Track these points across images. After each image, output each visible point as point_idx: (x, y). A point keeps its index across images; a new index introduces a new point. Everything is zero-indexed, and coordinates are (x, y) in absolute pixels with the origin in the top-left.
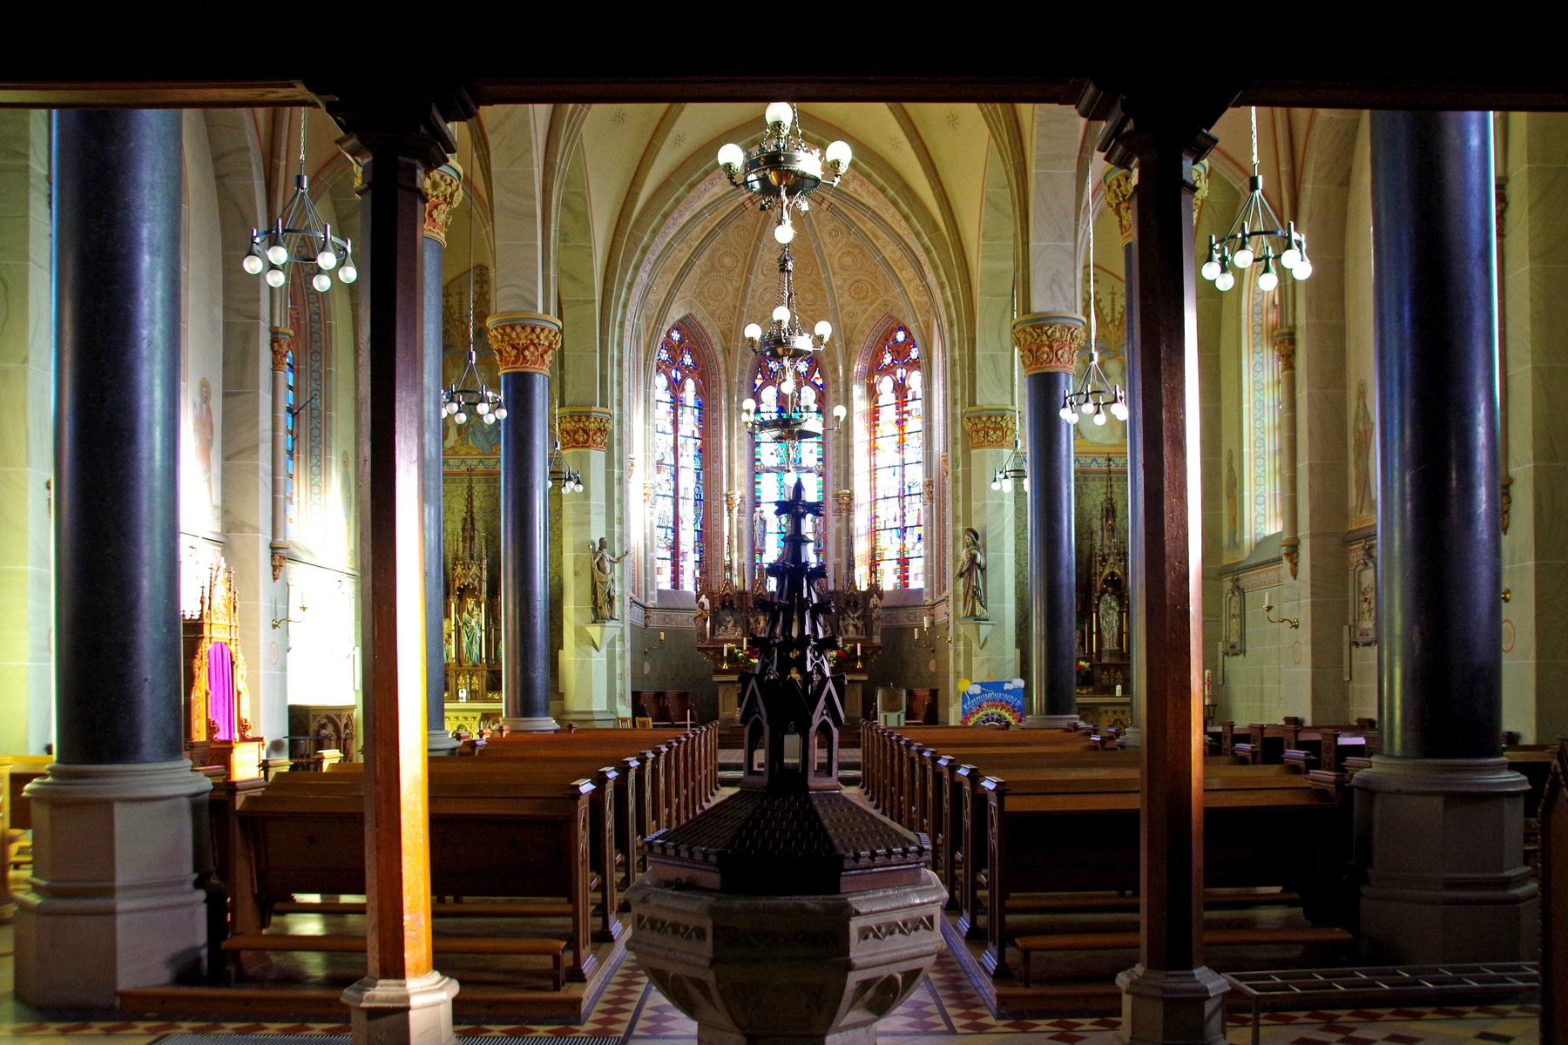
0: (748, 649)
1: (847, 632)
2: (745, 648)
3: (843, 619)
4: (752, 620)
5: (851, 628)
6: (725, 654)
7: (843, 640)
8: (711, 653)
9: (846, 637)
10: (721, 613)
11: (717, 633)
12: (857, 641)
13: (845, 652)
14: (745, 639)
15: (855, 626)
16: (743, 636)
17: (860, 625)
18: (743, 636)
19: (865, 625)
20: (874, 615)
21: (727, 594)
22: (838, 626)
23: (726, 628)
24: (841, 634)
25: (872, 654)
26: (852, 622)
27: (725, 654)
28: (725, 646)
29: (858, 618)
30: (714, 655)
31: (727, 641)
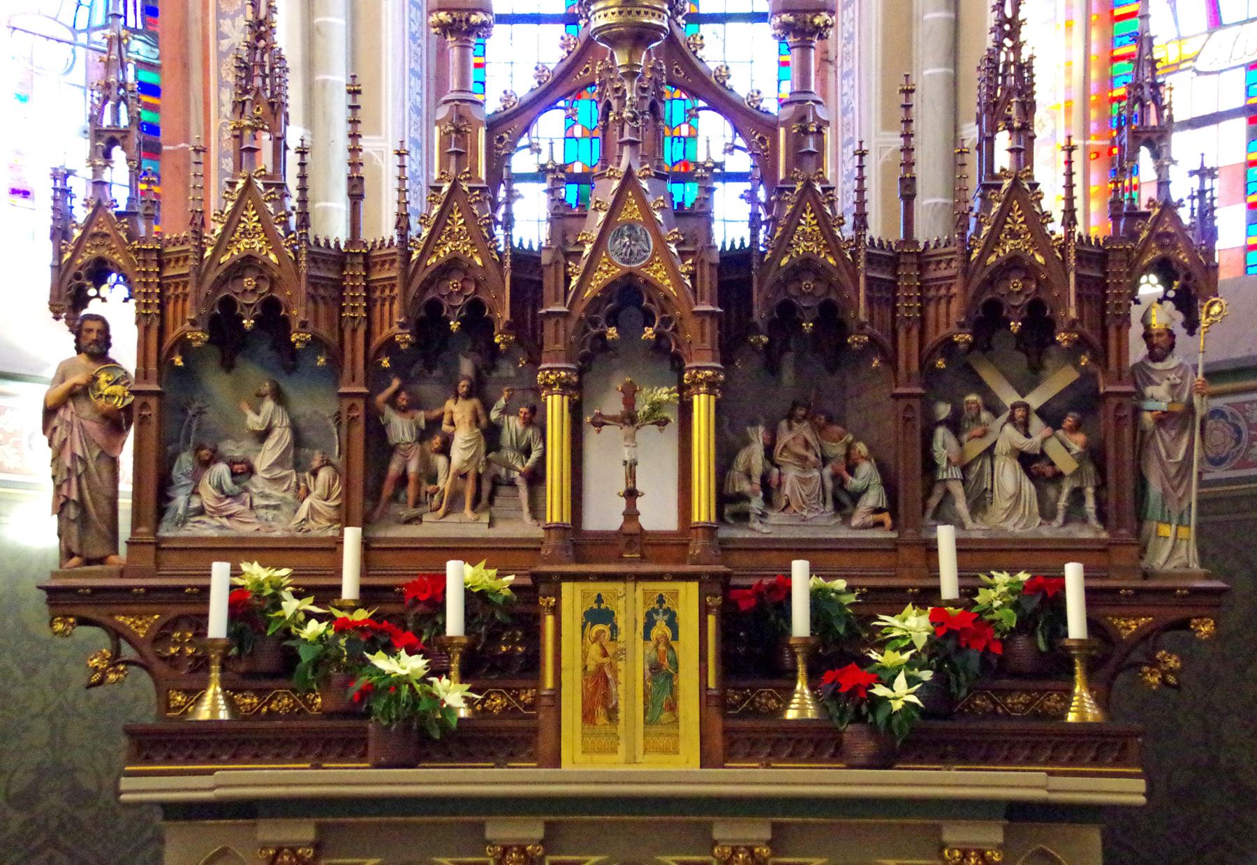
0: (368, 595)
1: (980, 502)
2: (349, 591)
3: (955, 425)
4: (401, 428)
5: (1008, 476)
6: (217, 625)
7: (964, 548)
8: (140, 626)
9: (976, 530)
10: (217, 384)
11: (180, 501)
12: (1072, 550)
13: (983, 622)
14: (352, 537)
15: (1027, 461)
16: (344, 518)
17: (1065, 463)
18: (344, 518)
19: (1095, 456)
20: (1159, 396)
21: (248, 262)
22: (930, 466)
23: (243, 471)
24: (941, 516)
25: (1146, 638)
26: (1009, 437)
27: (217, 625)
28: (220, 574)
29: (1051, 416)
30: (161, 636)
31: (236, 550)
